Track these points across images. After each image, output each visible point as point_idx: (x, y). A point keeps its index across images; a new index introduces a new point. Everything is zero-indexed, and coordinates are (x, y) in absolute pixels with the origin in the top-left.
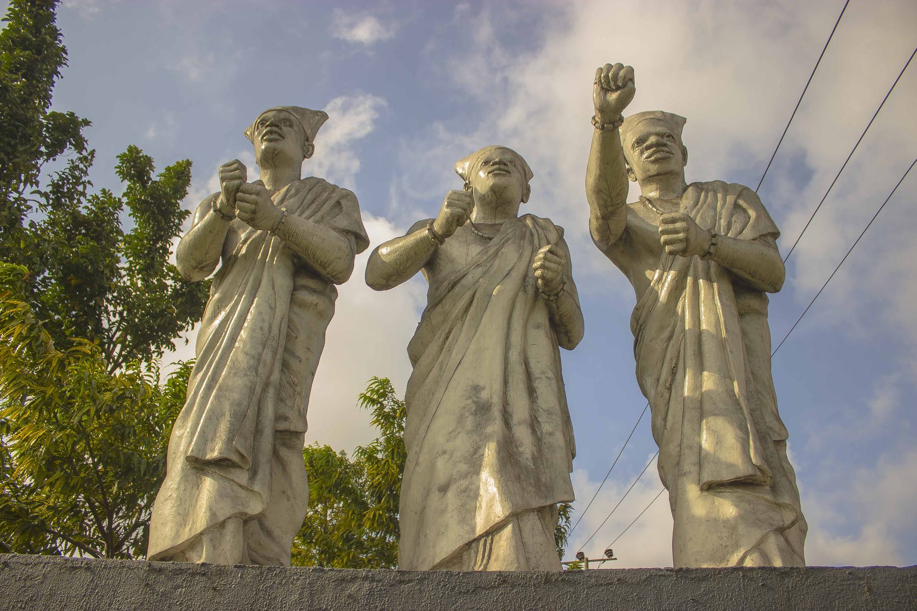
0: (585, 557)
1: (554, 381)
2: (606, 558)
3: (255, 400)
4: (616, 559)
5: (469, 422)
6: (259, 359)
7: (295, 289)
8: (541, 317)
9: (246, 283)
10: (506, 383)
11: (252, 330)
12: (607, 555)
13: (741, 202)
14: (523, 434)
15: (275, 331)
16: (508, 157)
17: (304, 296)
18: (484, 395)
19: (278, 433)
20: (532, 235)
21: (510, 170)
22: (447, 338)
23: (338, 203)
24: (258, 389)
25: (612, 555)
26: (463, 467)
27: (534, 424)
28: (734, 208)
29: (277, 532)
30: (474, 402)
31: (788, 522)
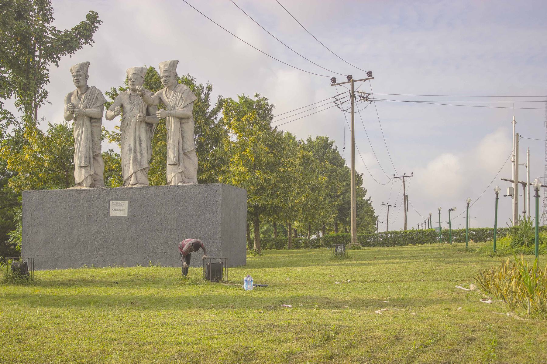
0: (353, 79)
1: (146, 142)
2: (368, 78)
3: (88, 153)
4: (373, 78)
5: (128, 152)
6: (87, 144)
7: (91, 123)
8: (143, 125)
9: (81, 124)
10: (135, 143)
11: (84, 137)
12: (368, 75)
13: (182, 96)
14: (138, 154)
15: (89, 136)
16: (135, 77)
17: (94, 124)
18: (131, 146)
19: (93, 156)
20: (140, 104)
21: (135, 83)
22: (125, 130)
23: (97, 97)
24: (88, 150)
25: (371, 76)
26: (128, 162)
27: (141, 152)
28: (181, 98)
29: (99, 174)
30: (130, 148)
31: (181, 171)
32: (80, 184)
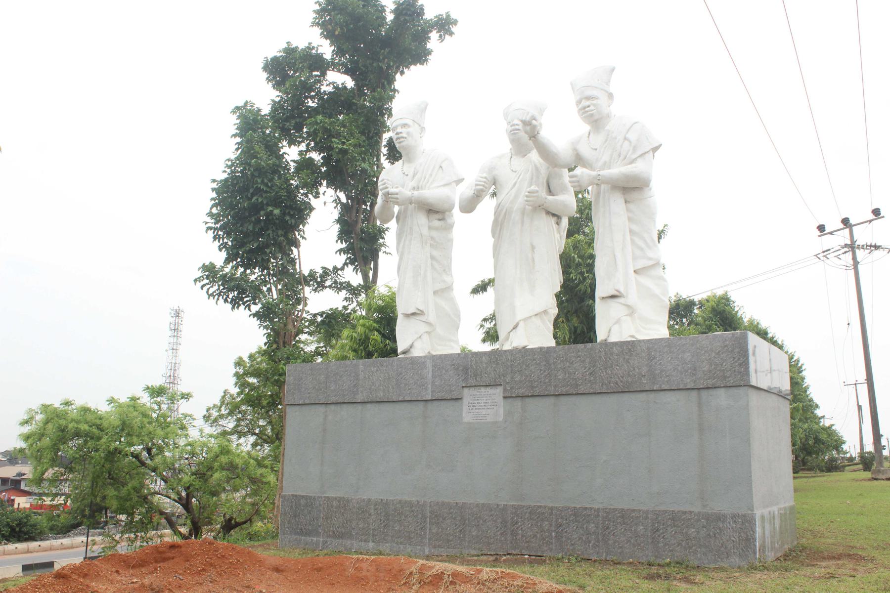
2: (874, 217)
4: (883, 217)
25: (880, 214)
32: (404, 353)
